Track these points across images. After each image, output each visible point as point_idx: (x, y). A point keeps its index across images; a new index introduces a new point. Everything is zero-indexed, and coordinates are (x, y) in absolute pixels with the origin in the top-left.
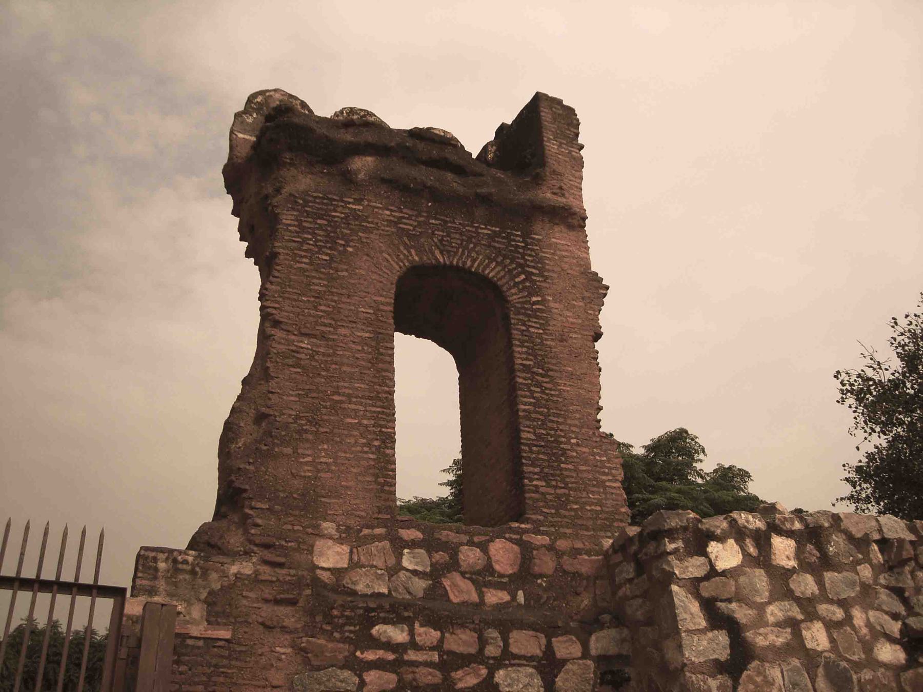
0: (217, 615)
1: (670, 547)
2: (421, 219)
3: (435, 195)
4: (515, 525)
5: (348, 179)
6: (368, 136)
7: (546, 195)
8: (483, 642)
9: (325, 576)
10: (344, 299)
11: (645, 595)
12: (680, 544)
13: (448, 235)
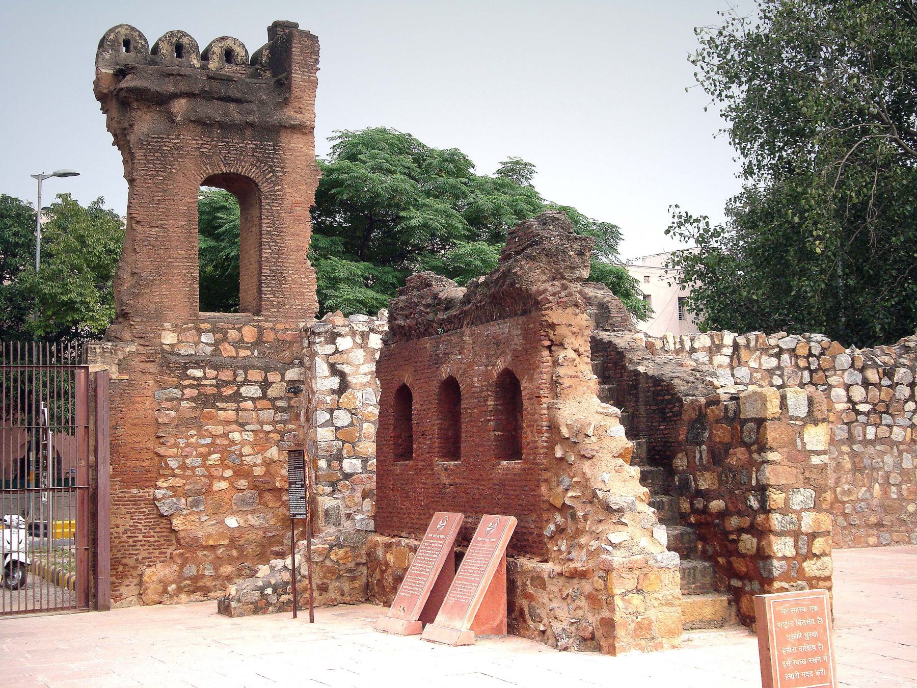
0: (123, 369)
1: (317, 340)
2: (214, 143)
3: (222, 126)
4: (256, 318)
5: (171, 118)
6: (183, 87)
7: (290, 114)
8: (235, 375)
9: (167, 348)
10: (171, 202)
11: (309, 356)
12: (322, 339)
13: (229, 153)
